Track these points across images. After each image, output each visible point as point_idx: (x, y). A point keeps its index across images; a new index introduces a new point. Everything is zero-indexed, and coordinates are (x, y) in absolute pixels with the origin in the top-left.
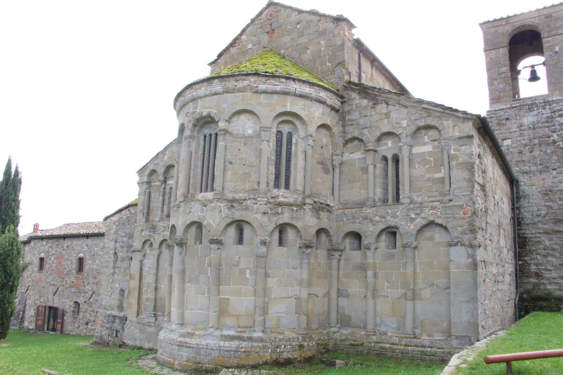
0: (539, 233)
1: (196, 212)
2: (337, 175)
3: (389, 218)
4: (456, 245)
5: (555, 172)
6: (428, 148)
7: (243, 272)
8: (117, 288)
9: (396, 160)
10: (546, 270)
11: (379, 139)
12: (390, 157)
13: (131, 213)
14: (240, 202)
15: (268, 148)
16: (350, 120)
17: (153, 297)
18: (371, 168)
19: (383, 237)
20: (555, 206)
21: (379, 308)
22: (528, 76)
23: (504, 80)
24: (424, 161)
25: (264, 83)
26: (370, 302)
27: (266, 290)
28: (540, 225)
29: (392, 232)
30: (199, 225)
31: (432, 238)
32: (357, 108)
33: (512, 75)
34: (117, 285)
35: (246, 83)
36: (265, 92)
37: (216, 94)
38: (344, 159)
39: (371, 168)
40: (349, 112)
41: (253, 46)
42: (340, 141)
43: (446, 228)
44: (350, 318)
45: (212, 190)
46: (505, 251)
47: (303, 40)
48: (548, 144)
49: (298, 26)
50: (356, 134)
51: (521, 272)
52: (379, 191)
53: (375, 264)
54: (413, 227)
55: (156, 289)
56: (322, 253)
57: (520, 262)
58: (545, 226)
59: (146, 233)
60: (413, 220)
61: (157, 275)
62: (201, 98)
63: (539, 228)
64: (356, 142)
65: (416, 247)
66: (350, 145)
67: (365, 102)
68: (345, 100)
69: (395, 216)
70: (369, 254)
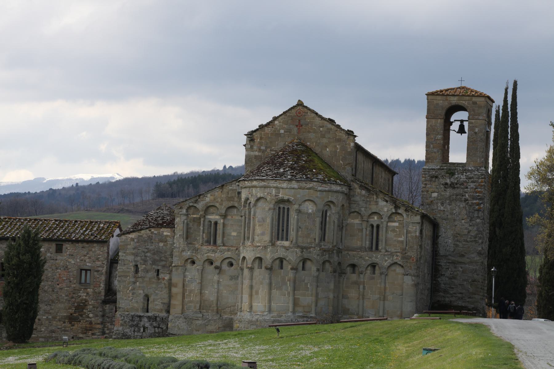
0: (449, 263)
1: (281, 253)
2: (344, 232)
3: (374, 259)
4: (407, 275)
5: (463, 221)
8: (140, 293)
9: (378, 226)
10: (450, 288)
11: (370, 215)
12: (375, 225)
13: (152, 233)
14: (307, 248)
15: (318, 220)
16: (353, 201)
17: (198, 299)
18: (364, 230)
19: (369, 268)
20: (460, 244)
21: (365, 305)
22: (457, 130)
23: (438, 143)
24: (393, 231)
25: (321, 187)
27: (317, 294)
28: (450, 257)
29: (373, 266)
30: (281, 260)
31: (395, 270)
32: (358, 194)
33: (445, 126)
34: (142, 292)
35: (311, 185)
36: (320, 191)
37: (293, 188)
38: (348, 222)
39: (364, 230)
40: (353, 196)
41: (285, 132)
43: (402, 267)
44: (349, 310)
45: (287, 240)
46: (427, 275)
48: (461, 201)
49: (321, 129)
50: (357, 210)
51: (435, 289)
52: (368, 242)
53: (364, 281)
54: (386, 264)
55: (201, 293)
56: (337, 274)
57: (435, 282)
58: (453, 258)
60: (386, 261)
61: (201, 283)
62: (283, 188)
63: (449, 259)
64: (355, 214)
65: (387, 275)
66: (352, 214)
67: (364, 192)
68: (352, 188)
69: (377, 258)
70: (362, 276)
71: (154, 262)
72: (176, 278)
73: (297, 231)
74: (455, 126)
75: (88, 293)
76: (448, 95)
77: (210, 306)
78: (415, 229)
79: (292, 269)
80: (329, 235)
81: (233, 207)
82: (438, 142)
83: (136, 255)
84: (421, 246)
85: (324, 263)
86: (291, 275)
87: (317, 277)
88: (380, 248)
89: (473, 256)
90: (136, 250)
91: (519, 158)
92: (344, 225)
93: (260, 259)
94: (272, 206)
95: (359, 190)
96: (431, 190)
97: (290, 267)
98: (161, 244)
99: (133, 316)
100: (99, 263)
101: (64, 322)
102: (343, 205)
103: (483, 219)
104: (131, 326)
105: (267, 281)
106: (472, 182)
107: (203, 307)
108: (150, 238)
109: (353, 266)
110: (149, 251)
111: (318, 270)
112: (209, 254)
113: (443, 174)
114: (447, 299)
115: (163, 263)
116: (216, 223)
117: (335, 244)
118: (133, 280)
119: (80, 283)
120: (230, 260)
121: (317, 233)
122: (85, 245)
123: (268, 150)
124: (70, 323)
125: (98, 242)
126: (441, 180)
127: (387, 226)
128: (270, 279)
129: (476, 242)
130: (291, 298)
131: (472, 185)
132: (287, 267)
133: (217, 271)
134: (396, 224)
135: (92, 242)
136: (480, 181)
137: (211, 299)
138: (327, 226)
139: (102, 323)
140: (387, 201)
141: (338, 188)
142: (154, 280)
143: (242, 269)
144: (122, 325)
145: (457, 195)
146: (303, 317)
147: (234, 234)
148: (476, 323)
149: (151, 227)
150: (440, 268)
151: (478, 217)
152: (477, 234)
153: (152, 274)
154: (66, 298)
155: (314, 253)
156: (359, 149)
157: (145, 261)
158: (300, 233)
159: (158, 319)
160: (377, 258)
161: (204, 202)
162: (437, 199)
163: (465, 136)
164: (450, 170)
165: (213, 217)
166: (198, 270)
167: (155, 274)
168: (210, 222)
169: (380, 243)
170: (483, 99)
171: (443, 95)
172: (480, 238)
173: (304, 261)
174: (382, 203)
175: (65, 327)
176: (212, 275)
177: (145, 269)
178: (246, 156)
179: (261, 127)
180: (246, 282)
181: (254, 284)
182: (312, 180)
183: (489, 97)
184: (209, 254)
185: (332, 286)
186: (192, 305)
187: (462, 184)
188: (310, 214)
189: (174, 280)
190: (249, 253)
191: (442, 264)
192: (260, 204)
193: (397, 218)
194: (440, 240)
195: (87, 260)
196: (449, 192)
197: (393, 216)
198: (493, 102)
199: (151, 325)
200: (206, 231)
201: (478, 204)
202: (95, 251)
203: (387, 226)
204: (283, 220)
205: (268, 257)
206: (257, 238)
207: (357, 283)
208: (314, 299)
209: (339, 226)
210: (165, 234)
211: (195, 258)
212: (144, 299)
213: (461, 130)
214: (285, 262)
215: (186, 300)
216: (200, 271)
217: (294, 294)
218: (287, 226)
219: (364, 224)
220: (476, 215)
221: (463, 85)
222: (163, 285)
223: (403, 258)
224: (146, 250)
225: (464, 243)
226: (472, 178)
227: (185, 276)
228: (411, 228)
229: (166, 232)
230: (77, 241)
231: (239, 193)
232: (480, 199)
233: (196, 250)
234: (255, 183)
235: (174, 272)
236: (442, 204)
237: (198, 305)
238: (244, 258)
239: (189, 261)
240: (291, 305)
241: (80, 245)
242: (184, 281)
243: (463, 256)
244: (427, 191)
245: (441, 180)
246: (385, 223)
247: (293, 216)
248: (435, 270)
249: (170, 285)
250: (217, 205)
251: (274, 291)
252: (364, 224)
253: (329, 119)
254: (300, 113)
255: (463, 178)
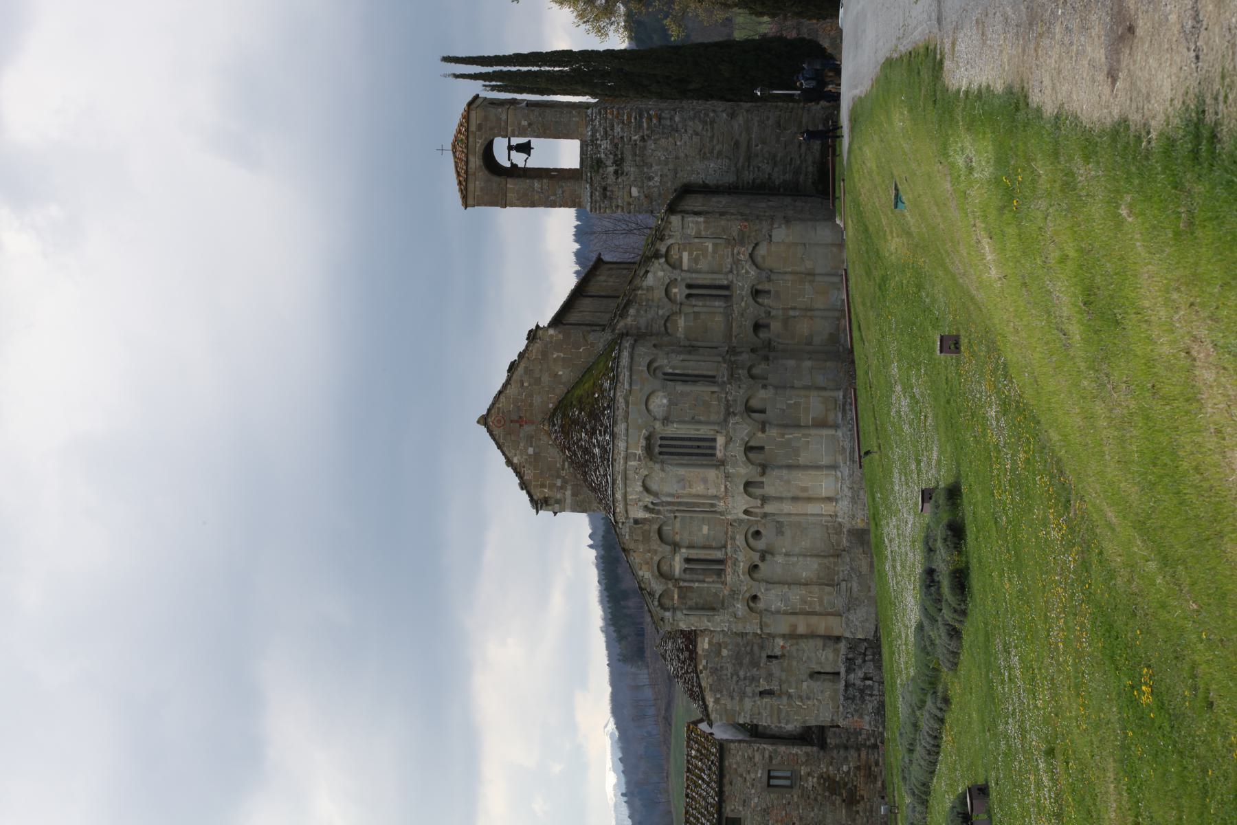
1: (737, 450)
2: (699, 344)
6: (685, 255)
7: (789, 406)
9: (689, 286)
11: (670, 299)
12: (688, 291)
13: (705, 668)
14: (728, 406)
15: (680, 388)
17: (816, 589)
18: (696, 309)
19: (760, 300)
20: (718, 148)
21: (822, 307)
22: (525, 156)
23: (546, 187)
24: (696, 260)
26: (817, 313)
28: (740, 164)
29: (756, 293)
30: (749, 449)
31: (763, 257)
33: (519, 176)
34: (805, 684)
35: (621, 400)
36: (631, 384)
39: (696, 309)
40: (639, 328)
42: (666, 339)
43: (757, 244)
45: (714, 440)
47: (546, 379)
48: (645, 147)
51: (793, 190)
52: (717, 304)
54: (753, 272)
55: (806, 584)
58: (741, 160)
59: (740, 607)
60: (747, 272)
61: (789, 584)
67: (632, 311)
69: (742, 287)
70: (773, 313)
71: (755, 664)
72: (782, 626)
73: (700, 422)
74: (519, 159)
75: (809, 774)
76: (466, 172)
77: (828, 568)
78: (694, 224)
79: (763, 431)
80: (705, 368)
81: (660, 531)
82: (545, 187)
83: (743, 695)
84: (722, 214)
85: (752, 377)
86: (773, 432)
87: (776, 387)
88: (726, 282)
89: (736, 127)
90: (735, 694)
91: (571, 51)
92: (687, 343)
93: (747, 485)
94: (657, 467)
95: (629, 319)
96: (626, 198)
97: (760, 434)
98: (725, 652)
99: (847, 698)
100: (757, 757)
101: (858, 812)
102: (655, 346)
103: (674, 110)
104: (863, 701)
105: (784, 472)
106: (612, 129)
107: (829, 581)
108: (714, 671)
109: (757, 327)
110: (736, 673)
111: (764, 387)
112: (741, 572)
113: (599, 178)
114: (810, 169)
115: (756, 648)
116: (688, 560)
117: (720, 359)
118: (785, 700)
119: (791, 787)
120: (749, 535)
121: (703, 389)
122: (726, 780)
123: (563, 473)
124: (858, 802)
125: (721, 759)
126: (609, 181)
127: (688, 271)
128: (780, 467)
129: (713, 122)
130: (813, 432)
131: (618, 129)
132: (760, 439)
133: (768, 557)
134: (685, 255)
135: (721, 768)
136: (610, 116)
137: (816, 566)
138: (690, 372)
139: (858, 750)
140: (647, 272)
141: (626, 354)
142: (785, 664)
143: (765, 515)
144: (861, 716)
145: (635, 155)
146: (844, 411)
147: (705, 529)
148: (850, 120)
149: (695, 671)
150: (758, 181)
151: (671, 119)
152: (700, 120)
153: (775, 666)
154: (816, 810)
155: (737, 393)
156: (557, 320)
157: (753, 679)
158: (702, 418)
159: (850, 656)
160: (742, 287)
161: (652, 581)
162: (642, 187)
163: (535, 142)
164: (592, 167)
165: (678, 566)
166: (767, 590)
167: (775, 661)
168: (685, 570)
169: (717, 283)
170: (473, 114)
171: (466, 180)
172: (707, 115)
173: (749, 410)
174: (650, 280)
175: (865, 811)
176: (775, 567)
177: (766, 679)
178: (574, 510)
179: (524, 485)
180: (787, 507)
181: (790, 495)
182: (613, 400)
183: (470, 104)
184: (741, 572)
185: (791, 363)
186: (826, 598)
187: (616, 146)
188: (670, 400)
189: (784, 628)
190: (738, 505)
191: (751, 177)
192: (654, 487)
193: (674, 254)
194: (711, 181)
195: (753, 776)
196: (629, 167)
197: (672, 261)
198: (477, 96)
199: (860, 667)
200: (701, 577)
201: (650, 118)
202: (737, 763)
203: (688, 271)
204: (681, 447)
205: (743, 471)
206: (712, 491)
207: (786, 321)
208: (813, 393)
209: (690, 353)
210: (706, 646)
211: (747, 595)
212: (817, 680)
213: (525, 149)
214: (752, 443)
215: (818, 609)
216: (770, 586)
217: (807, 427)
218: (690, 439)
219: (686, 309)
220: (668, 122)
221: (450, 147)
222: (794, 649)
223: (742, 243)
224: (735, 678)
225: (715, 141)
226: (605, 129)
227: (778, 612)
228: (691, 231)
229: (704, 644)
230: (720, 793)
231: (636, 521)
232: (641, 116)
233: (733, 593)
234: (619, 496)
235: (771, 630)
236: (650, 179)
237: (828, 589)
238: (746, 512)
239: (752, 604)
240: (825, 432)
241: (727, 788)
242: (786, 613)
243: (737, 144)
244: (629, 204)
245: (609, 181)
246: (684, 274)
247: (674, 430)
248: (762, 189)
249: (793, 636)
250: (656, 559)
251: (801, 461)
252: (686, 309)
253: (509, 371)
254: (499, 421)
255: (605, 145)
